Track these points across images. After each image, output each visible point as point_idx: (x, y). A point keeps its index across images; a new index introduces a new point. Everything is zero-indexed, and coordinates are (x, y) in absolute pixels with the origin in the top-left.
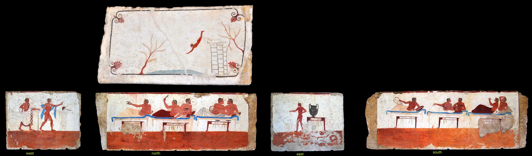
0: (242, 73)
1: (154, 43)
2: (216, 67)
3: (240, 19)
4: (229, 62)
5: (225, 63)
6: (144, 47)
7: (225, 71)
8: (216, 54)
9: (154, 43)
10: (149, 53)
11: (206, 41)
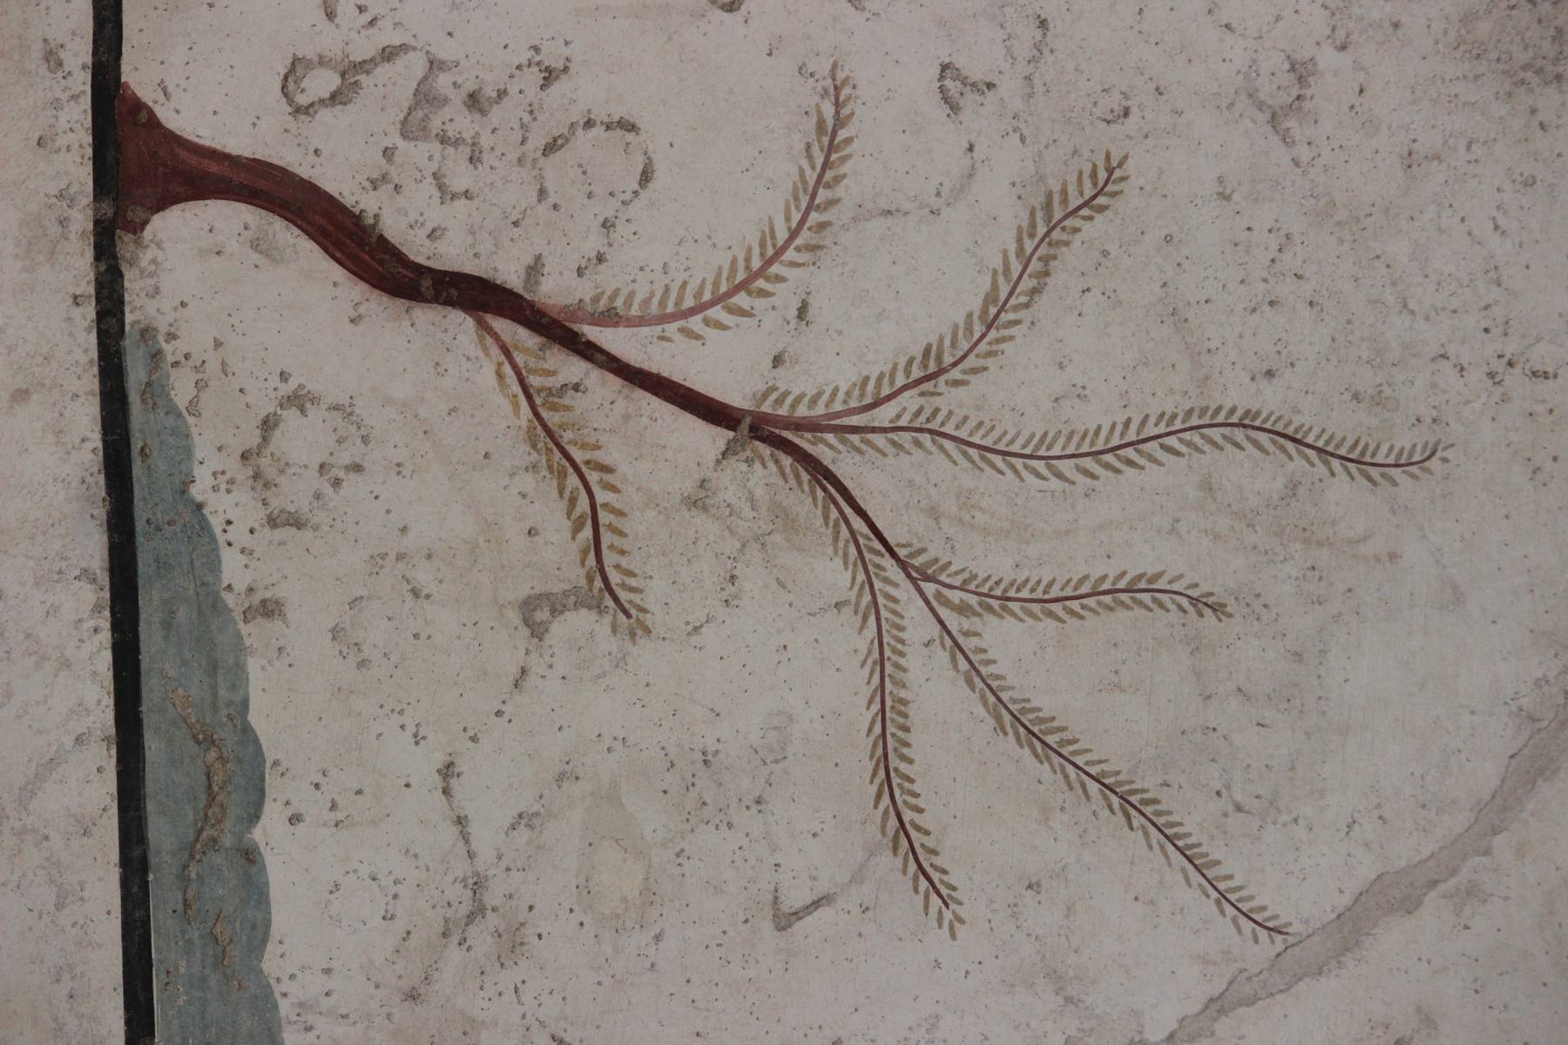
1: (1130, 523)
6: (1000, 207)
9: (1130, 523)
10: (823, 374)
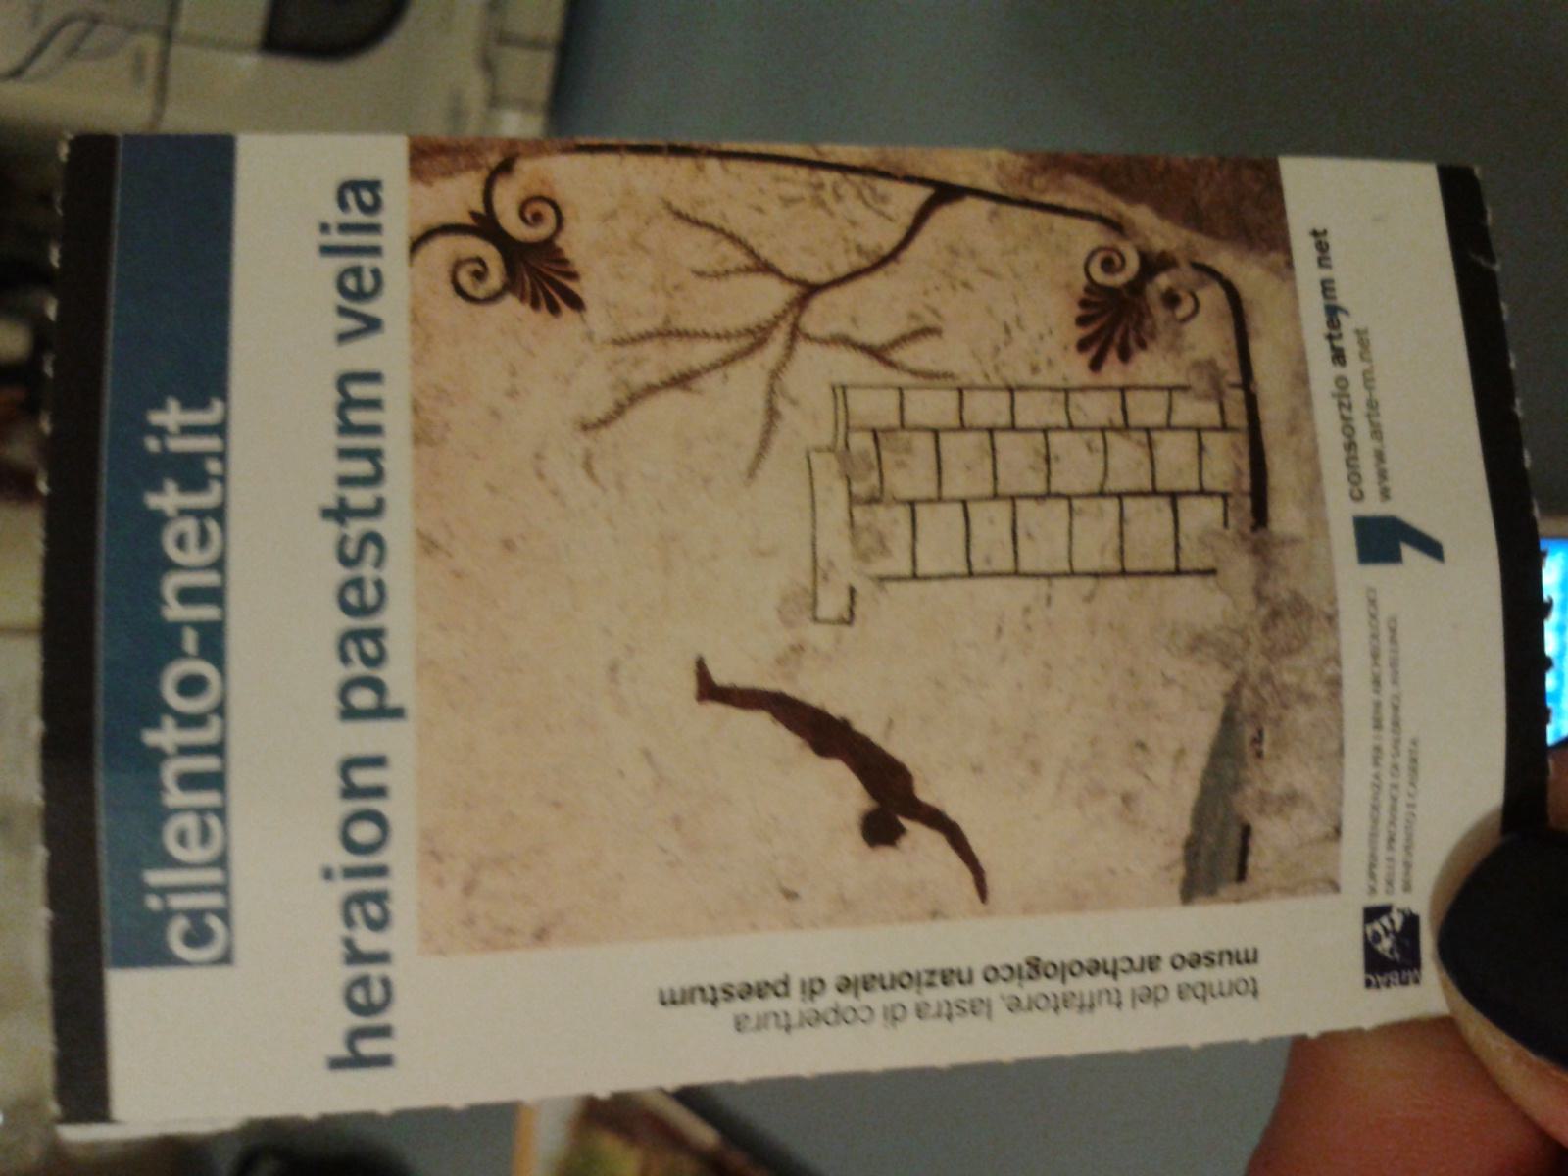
0: (1195, 219)
2: (1150, 522)
3: (540, 204)
4: (1076, 368)
5: (1097, 408)
7: (1190, 410)
8: (991, 521)
11: (820, 636)
